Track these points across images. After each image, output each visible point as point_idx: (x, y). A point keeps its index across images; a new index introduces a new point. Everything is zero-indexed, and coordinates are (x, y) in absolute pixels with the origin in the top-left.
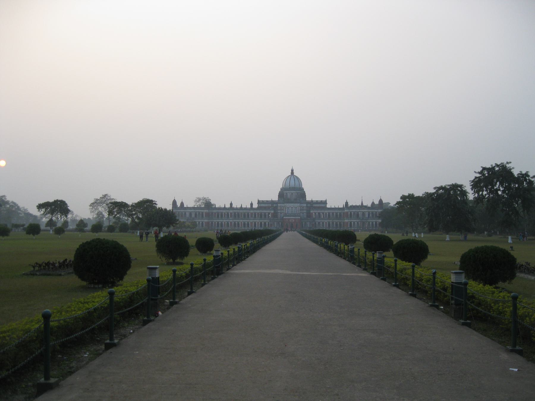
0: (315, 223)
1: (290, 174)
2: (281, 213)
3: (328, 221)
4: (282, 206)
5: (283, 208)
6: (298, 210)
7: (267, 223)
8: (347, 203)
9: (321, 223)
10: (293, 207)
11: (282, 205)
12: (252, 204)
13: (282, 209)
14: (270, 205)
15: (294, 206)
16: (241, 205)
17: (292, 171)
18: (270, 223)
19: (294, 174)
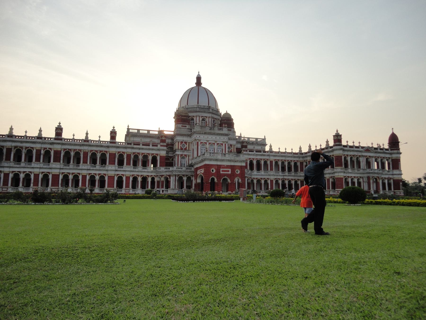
0: (252, 181)
1: (195, 85)
2: (183, 157)
3: (276, 177)
4: (186, 143)
5: (188, 146)
6: (224, 148)
7: (150, 180)
8: (338, 138)
9: (263, 182)
10: (214, 144)
11: (185, 139)
12: (113, 134)
13: (186, 149)
14: (157, 141)
15: (216, 141)
16: (87, 134)
17: (199, 79)
18: (156, 179)
19: (202, 86)
